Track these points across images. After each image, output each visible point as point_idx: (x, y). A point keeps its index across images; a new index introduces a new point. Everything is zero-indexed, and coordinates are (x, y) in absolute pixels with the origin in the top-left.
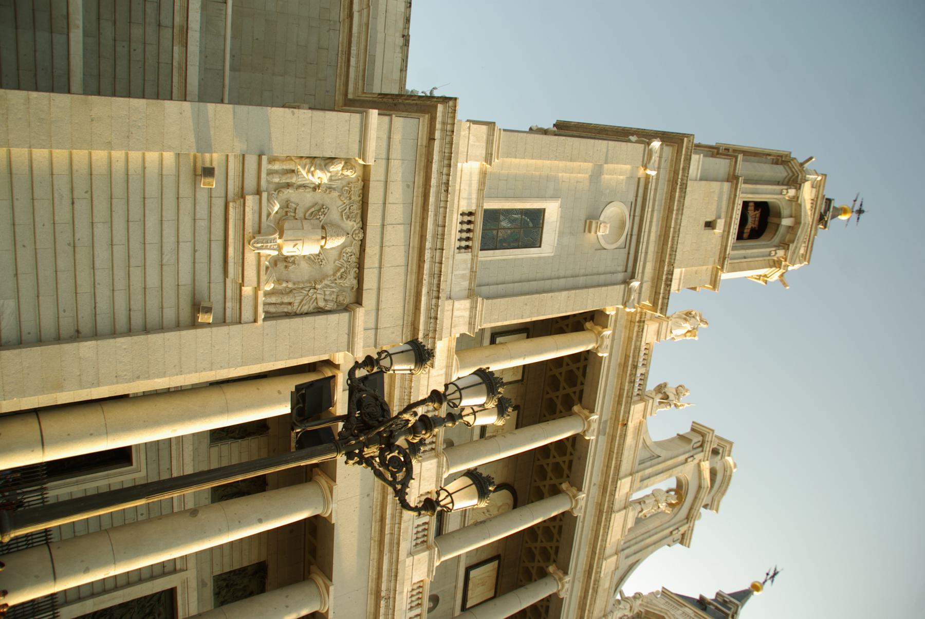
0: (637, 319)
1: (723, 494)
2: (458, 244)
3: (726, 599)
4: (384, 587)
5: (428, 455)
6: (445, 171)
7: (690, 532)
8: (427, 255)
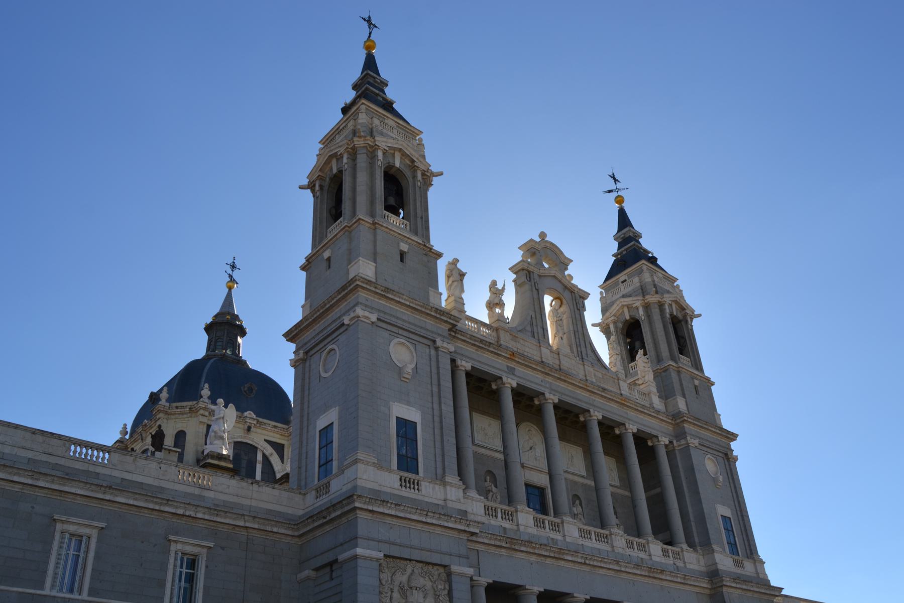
0: (453, 334)
2: (417, 491)
3: (621, 236)
4: (580, 560)
5: (515, 518)
6: (389, 505)
7: (580, 292)
8: (429, 520)
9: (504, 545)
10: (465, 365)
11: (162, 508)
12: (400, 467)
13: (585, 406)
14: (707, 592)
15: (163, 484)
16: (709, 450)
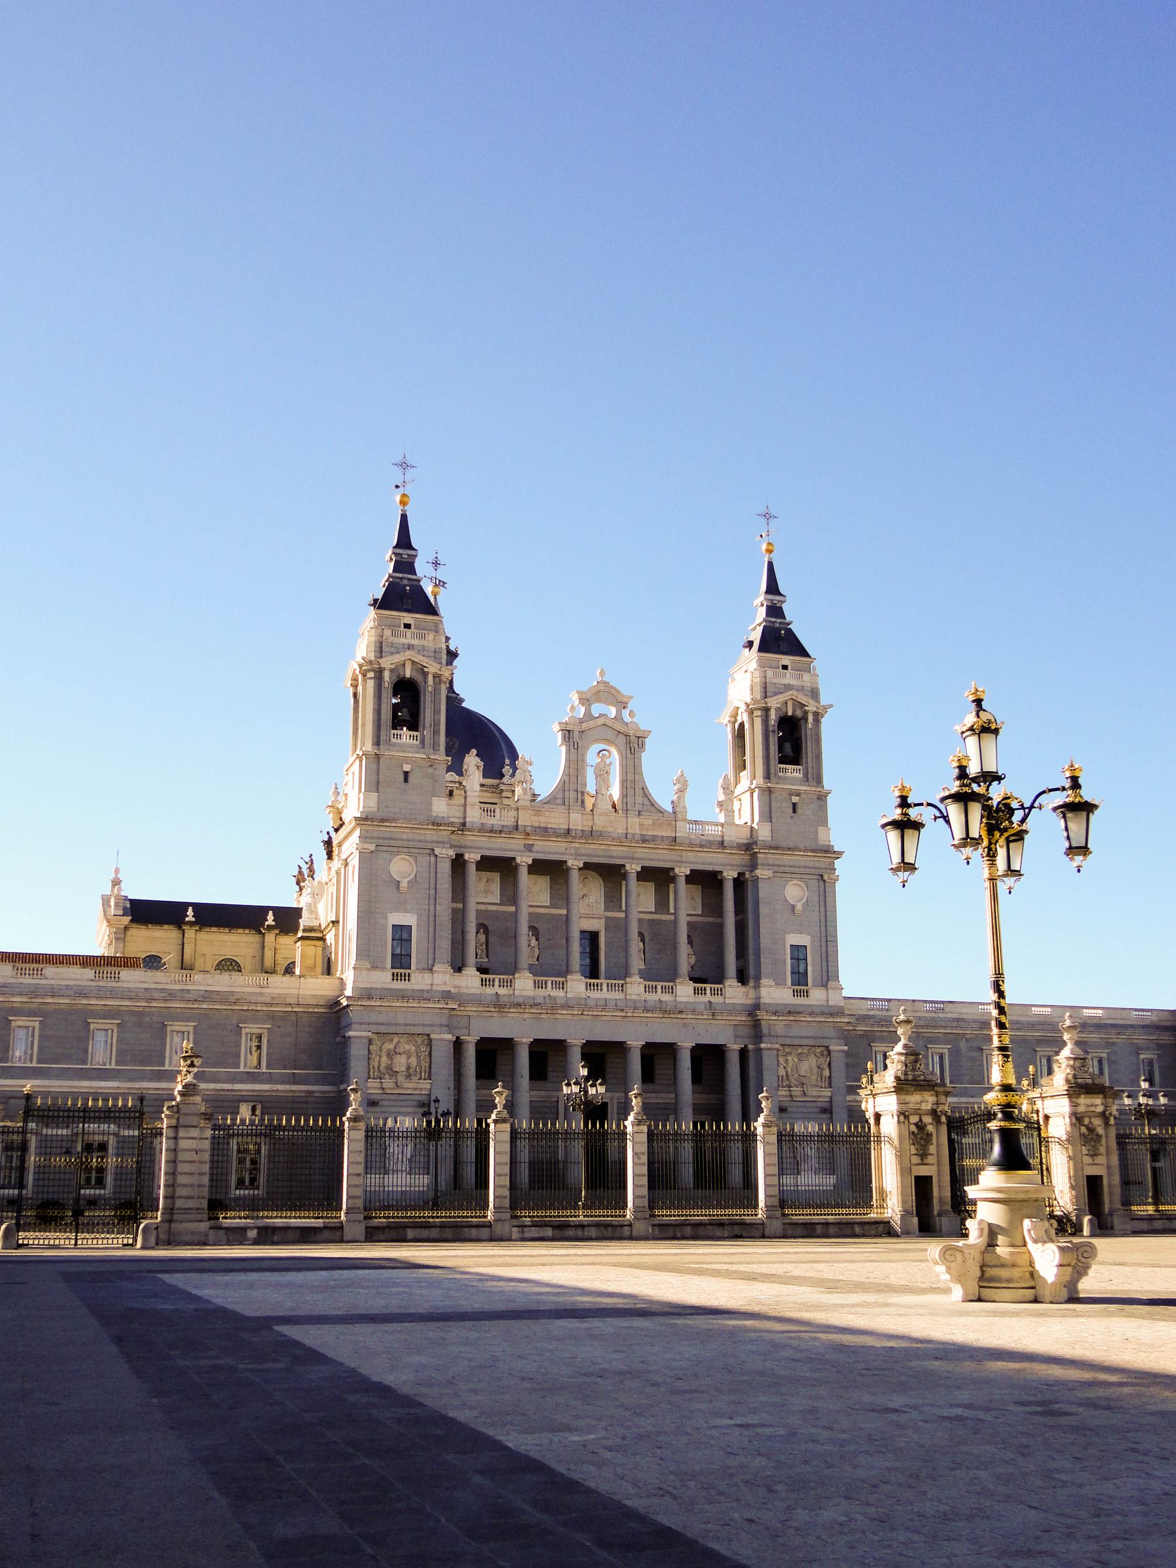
0: (461, 832)
1: (618, 691)
4: (577, 1013)
8: (410, 1005)
9: (492, 1010)
10: (472, 857)
11: (232, 1008)
12: (392, 968)
13: (619, 862)
14: (752, 1023)
15: (233, 989)
16: (794, 876)
